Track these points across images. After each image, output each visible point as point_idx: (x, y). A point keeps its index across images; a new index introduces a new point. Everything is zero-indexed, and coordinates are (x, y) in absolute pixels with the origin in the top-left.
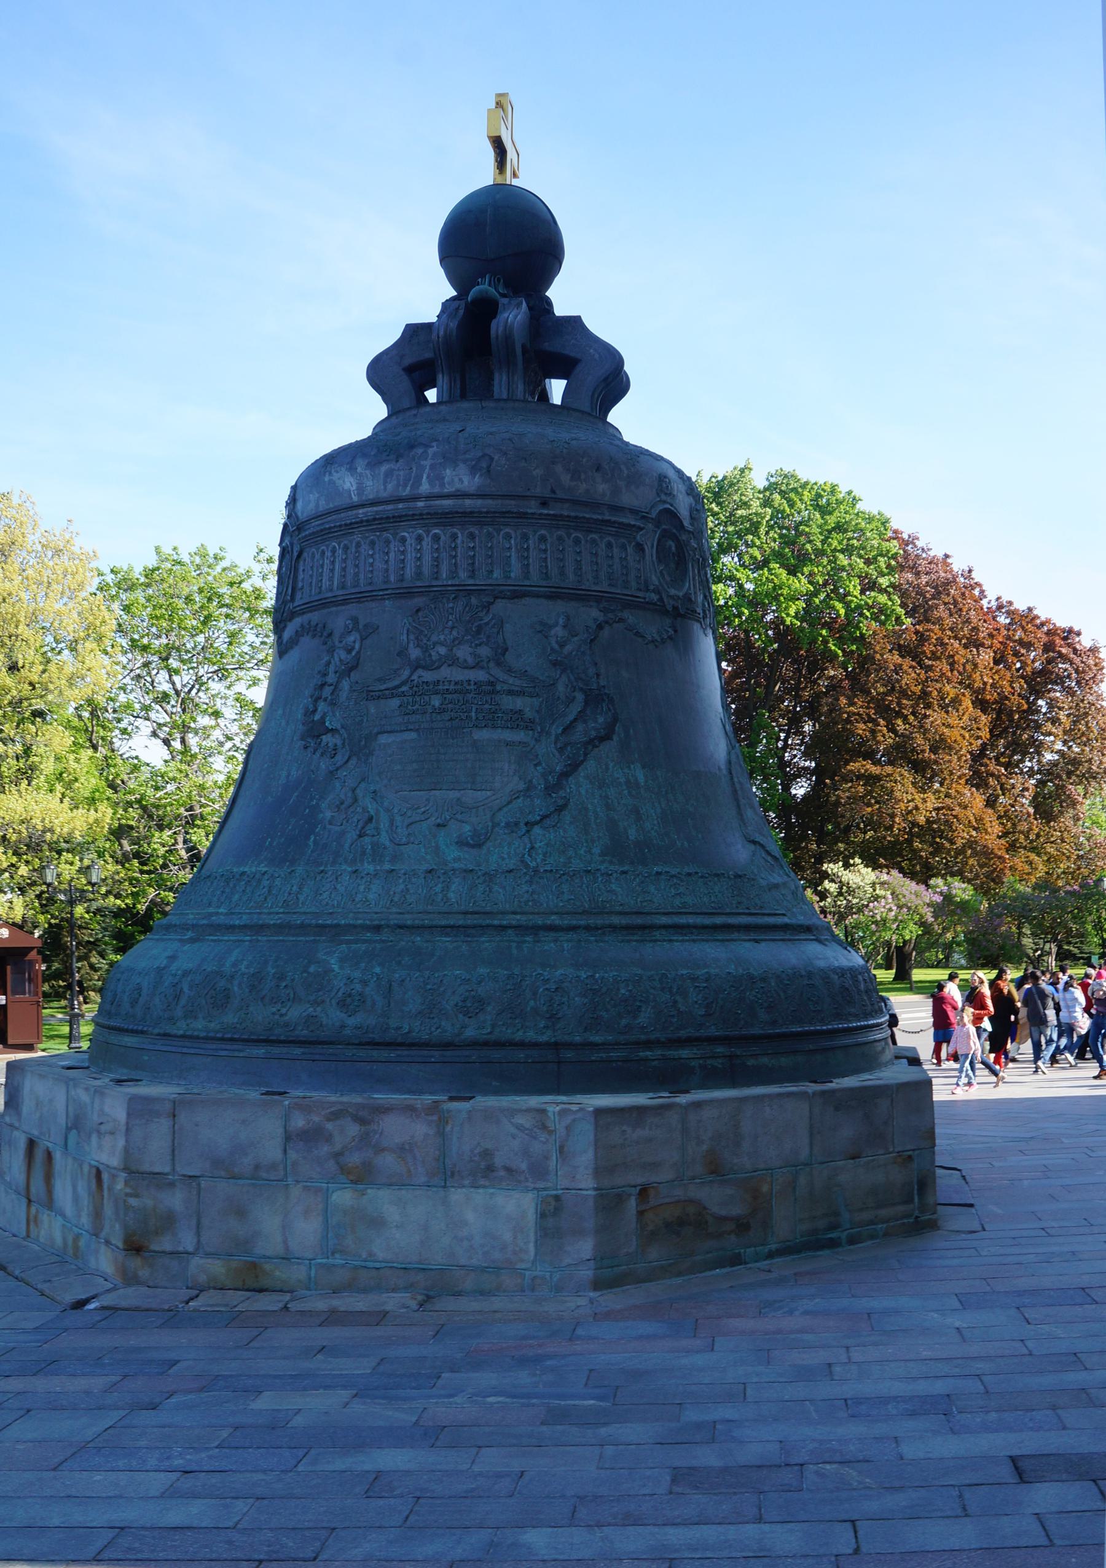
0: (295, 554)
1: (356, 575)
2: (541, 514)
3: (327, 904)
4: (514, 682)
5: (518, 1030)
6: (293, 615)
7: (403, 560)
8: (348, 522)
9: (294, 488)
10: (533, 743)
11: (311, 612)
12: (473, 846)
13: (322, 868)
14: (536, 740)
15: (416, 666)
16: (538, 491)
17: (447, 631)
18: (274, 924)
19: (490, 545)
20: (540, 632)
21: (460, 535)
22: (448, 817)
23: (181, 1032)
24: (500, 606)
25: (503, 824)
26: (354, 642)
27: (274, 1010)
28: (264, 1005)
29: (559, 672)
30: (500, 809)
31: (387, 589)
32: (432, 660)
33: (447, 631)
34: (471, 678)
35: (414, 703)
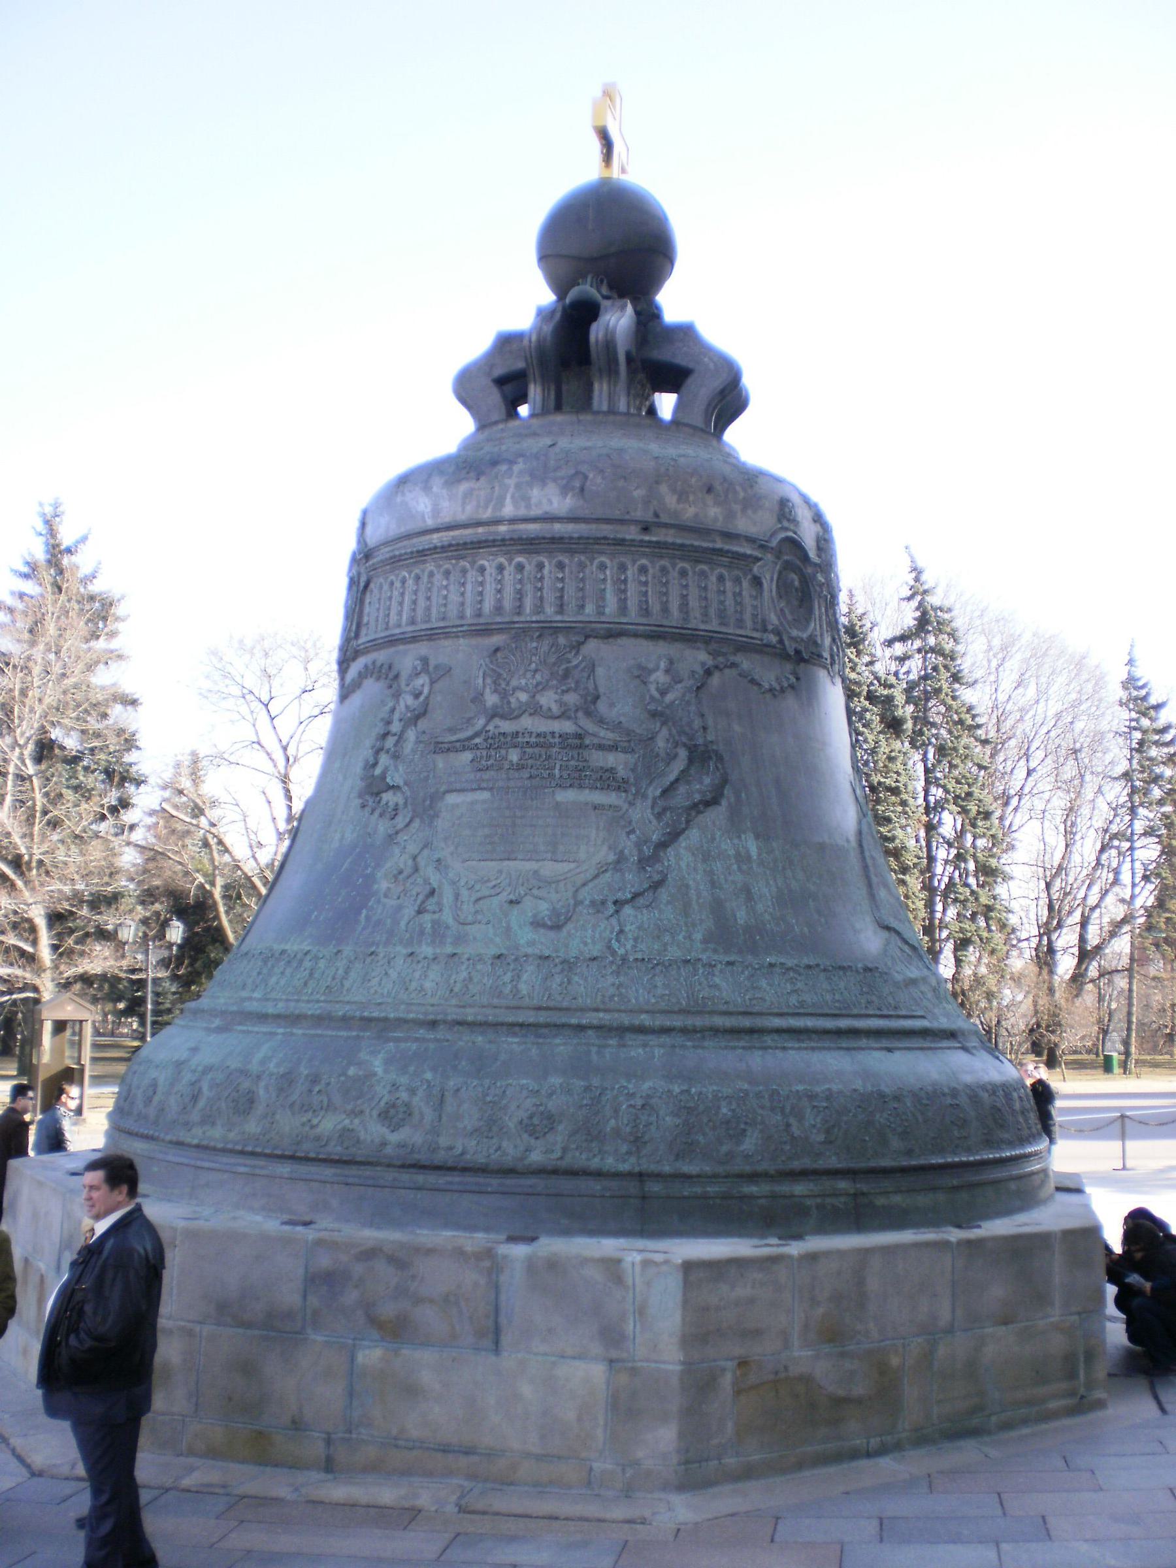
0: (362, 584)
1: (428, 609)
2: (641, 541)
4: (607, 736)
5: (595, 1156)
6: (357, 654)
8: (421, 548)
9: (365, 513)
10: (625, 806)
11: (377, 650)
12: (551, 928)
13: (373, 949)
15: (493, 715)
16: (638, 514)
17: (529, 675)
18: (312, 1015)
19: (581, 575)
20: (638, 677)
21: (546, 564)
22: (522, 893)
23: (195, 1142)
24: (591, 646)
25: (587, 902)
26: (423, 685)
27: (305, 1119)
28: (293, 1114)
30: (584, 885)
31: (462, 626)
32: (510, 708)
33: (529, 675)
35: (489, 757)
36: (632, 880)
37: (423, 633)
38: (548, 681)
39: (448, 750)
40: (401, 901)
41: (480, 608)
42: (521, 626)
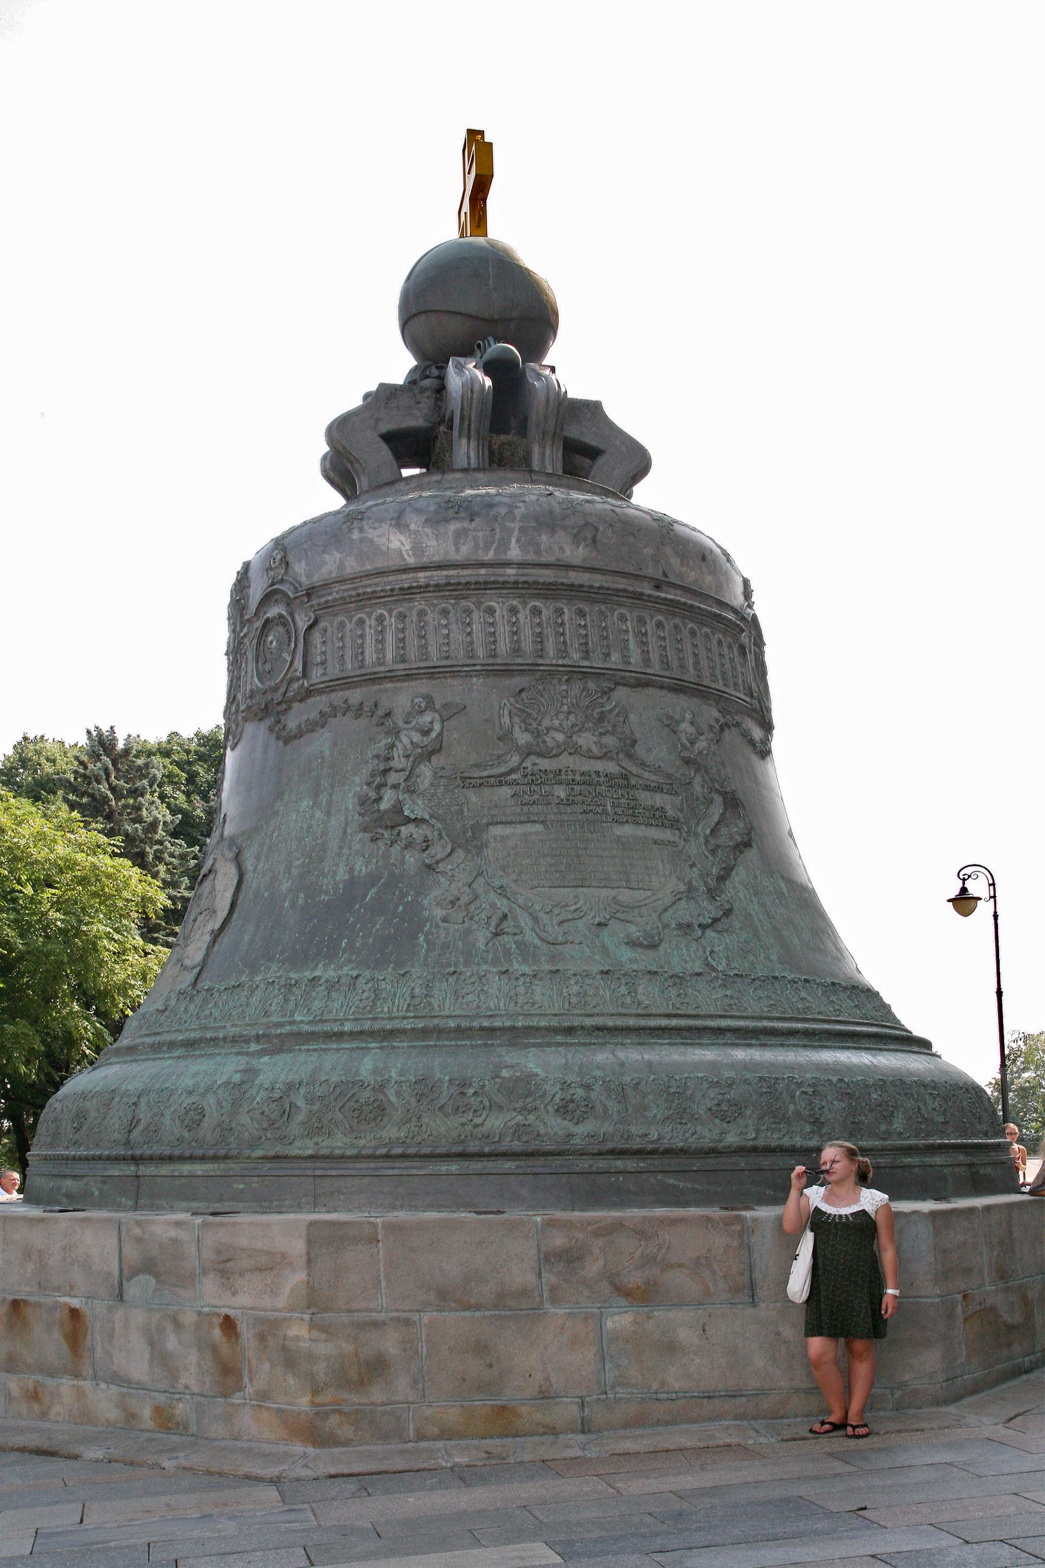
2: (658, 597)
3: (478, 1007)
7: (494, 633)
13: (452, 969)
14: (685, 840)
17: (562, 716)
18: (413, 1029)
22: (608, 917)
29: (693, 772)
32: (547, 746)
33: (562, 716)
34: (600, 769)
35: (532, 793)
36: (709, 910)
37: (422, 671)
38: (583, 723)
39: (481, 784)
40: (466, 925)
41: (495, 649)
42: (547, 668)
